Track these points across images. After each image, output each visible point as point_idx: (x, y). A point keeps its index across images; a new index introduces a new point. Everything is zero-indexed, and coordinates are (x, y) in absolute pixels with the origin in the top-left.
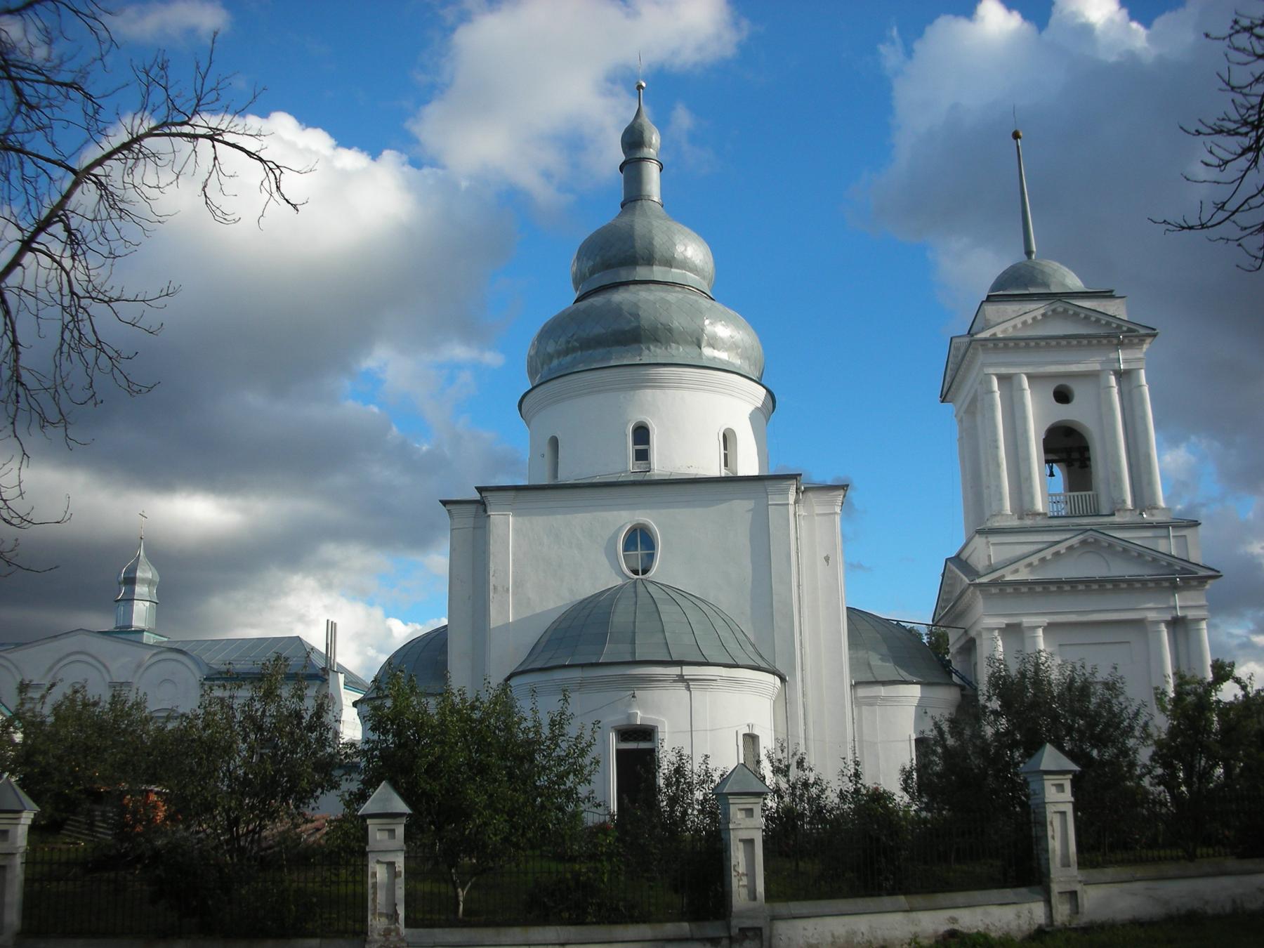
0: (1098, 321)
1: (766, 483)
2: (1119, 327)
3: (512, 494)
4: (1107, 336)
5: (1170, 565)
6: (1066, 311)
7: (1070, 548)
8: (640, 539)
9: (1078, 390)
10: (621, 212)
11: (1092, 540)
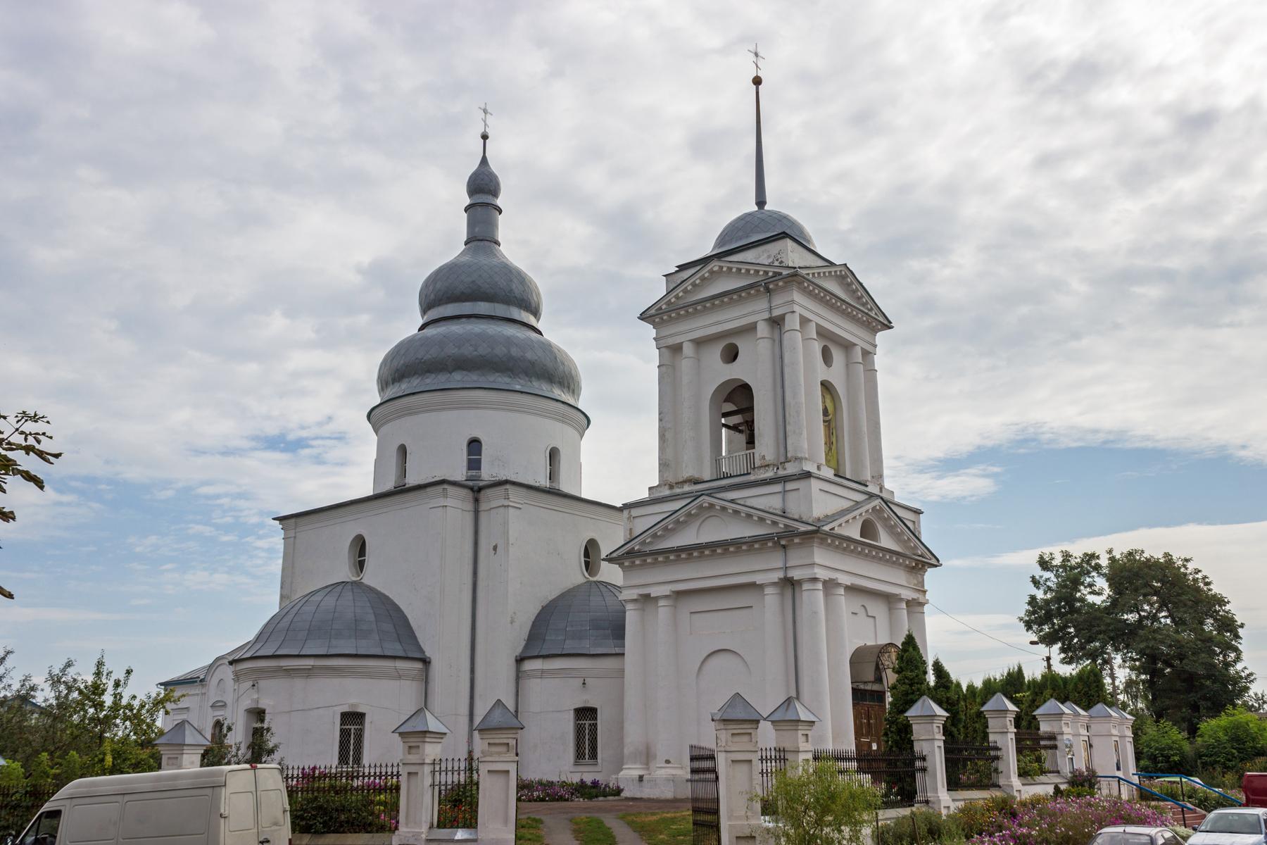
0: (748, 271)
1: (428, 489)
2: (766, 273)
3: (293, 520)
4: (751, 286)
5: (775, 523)
6: (721, 267)
7: (689, 515)
8: (360, 546)
10: (465, 249)
11: (707, 505)
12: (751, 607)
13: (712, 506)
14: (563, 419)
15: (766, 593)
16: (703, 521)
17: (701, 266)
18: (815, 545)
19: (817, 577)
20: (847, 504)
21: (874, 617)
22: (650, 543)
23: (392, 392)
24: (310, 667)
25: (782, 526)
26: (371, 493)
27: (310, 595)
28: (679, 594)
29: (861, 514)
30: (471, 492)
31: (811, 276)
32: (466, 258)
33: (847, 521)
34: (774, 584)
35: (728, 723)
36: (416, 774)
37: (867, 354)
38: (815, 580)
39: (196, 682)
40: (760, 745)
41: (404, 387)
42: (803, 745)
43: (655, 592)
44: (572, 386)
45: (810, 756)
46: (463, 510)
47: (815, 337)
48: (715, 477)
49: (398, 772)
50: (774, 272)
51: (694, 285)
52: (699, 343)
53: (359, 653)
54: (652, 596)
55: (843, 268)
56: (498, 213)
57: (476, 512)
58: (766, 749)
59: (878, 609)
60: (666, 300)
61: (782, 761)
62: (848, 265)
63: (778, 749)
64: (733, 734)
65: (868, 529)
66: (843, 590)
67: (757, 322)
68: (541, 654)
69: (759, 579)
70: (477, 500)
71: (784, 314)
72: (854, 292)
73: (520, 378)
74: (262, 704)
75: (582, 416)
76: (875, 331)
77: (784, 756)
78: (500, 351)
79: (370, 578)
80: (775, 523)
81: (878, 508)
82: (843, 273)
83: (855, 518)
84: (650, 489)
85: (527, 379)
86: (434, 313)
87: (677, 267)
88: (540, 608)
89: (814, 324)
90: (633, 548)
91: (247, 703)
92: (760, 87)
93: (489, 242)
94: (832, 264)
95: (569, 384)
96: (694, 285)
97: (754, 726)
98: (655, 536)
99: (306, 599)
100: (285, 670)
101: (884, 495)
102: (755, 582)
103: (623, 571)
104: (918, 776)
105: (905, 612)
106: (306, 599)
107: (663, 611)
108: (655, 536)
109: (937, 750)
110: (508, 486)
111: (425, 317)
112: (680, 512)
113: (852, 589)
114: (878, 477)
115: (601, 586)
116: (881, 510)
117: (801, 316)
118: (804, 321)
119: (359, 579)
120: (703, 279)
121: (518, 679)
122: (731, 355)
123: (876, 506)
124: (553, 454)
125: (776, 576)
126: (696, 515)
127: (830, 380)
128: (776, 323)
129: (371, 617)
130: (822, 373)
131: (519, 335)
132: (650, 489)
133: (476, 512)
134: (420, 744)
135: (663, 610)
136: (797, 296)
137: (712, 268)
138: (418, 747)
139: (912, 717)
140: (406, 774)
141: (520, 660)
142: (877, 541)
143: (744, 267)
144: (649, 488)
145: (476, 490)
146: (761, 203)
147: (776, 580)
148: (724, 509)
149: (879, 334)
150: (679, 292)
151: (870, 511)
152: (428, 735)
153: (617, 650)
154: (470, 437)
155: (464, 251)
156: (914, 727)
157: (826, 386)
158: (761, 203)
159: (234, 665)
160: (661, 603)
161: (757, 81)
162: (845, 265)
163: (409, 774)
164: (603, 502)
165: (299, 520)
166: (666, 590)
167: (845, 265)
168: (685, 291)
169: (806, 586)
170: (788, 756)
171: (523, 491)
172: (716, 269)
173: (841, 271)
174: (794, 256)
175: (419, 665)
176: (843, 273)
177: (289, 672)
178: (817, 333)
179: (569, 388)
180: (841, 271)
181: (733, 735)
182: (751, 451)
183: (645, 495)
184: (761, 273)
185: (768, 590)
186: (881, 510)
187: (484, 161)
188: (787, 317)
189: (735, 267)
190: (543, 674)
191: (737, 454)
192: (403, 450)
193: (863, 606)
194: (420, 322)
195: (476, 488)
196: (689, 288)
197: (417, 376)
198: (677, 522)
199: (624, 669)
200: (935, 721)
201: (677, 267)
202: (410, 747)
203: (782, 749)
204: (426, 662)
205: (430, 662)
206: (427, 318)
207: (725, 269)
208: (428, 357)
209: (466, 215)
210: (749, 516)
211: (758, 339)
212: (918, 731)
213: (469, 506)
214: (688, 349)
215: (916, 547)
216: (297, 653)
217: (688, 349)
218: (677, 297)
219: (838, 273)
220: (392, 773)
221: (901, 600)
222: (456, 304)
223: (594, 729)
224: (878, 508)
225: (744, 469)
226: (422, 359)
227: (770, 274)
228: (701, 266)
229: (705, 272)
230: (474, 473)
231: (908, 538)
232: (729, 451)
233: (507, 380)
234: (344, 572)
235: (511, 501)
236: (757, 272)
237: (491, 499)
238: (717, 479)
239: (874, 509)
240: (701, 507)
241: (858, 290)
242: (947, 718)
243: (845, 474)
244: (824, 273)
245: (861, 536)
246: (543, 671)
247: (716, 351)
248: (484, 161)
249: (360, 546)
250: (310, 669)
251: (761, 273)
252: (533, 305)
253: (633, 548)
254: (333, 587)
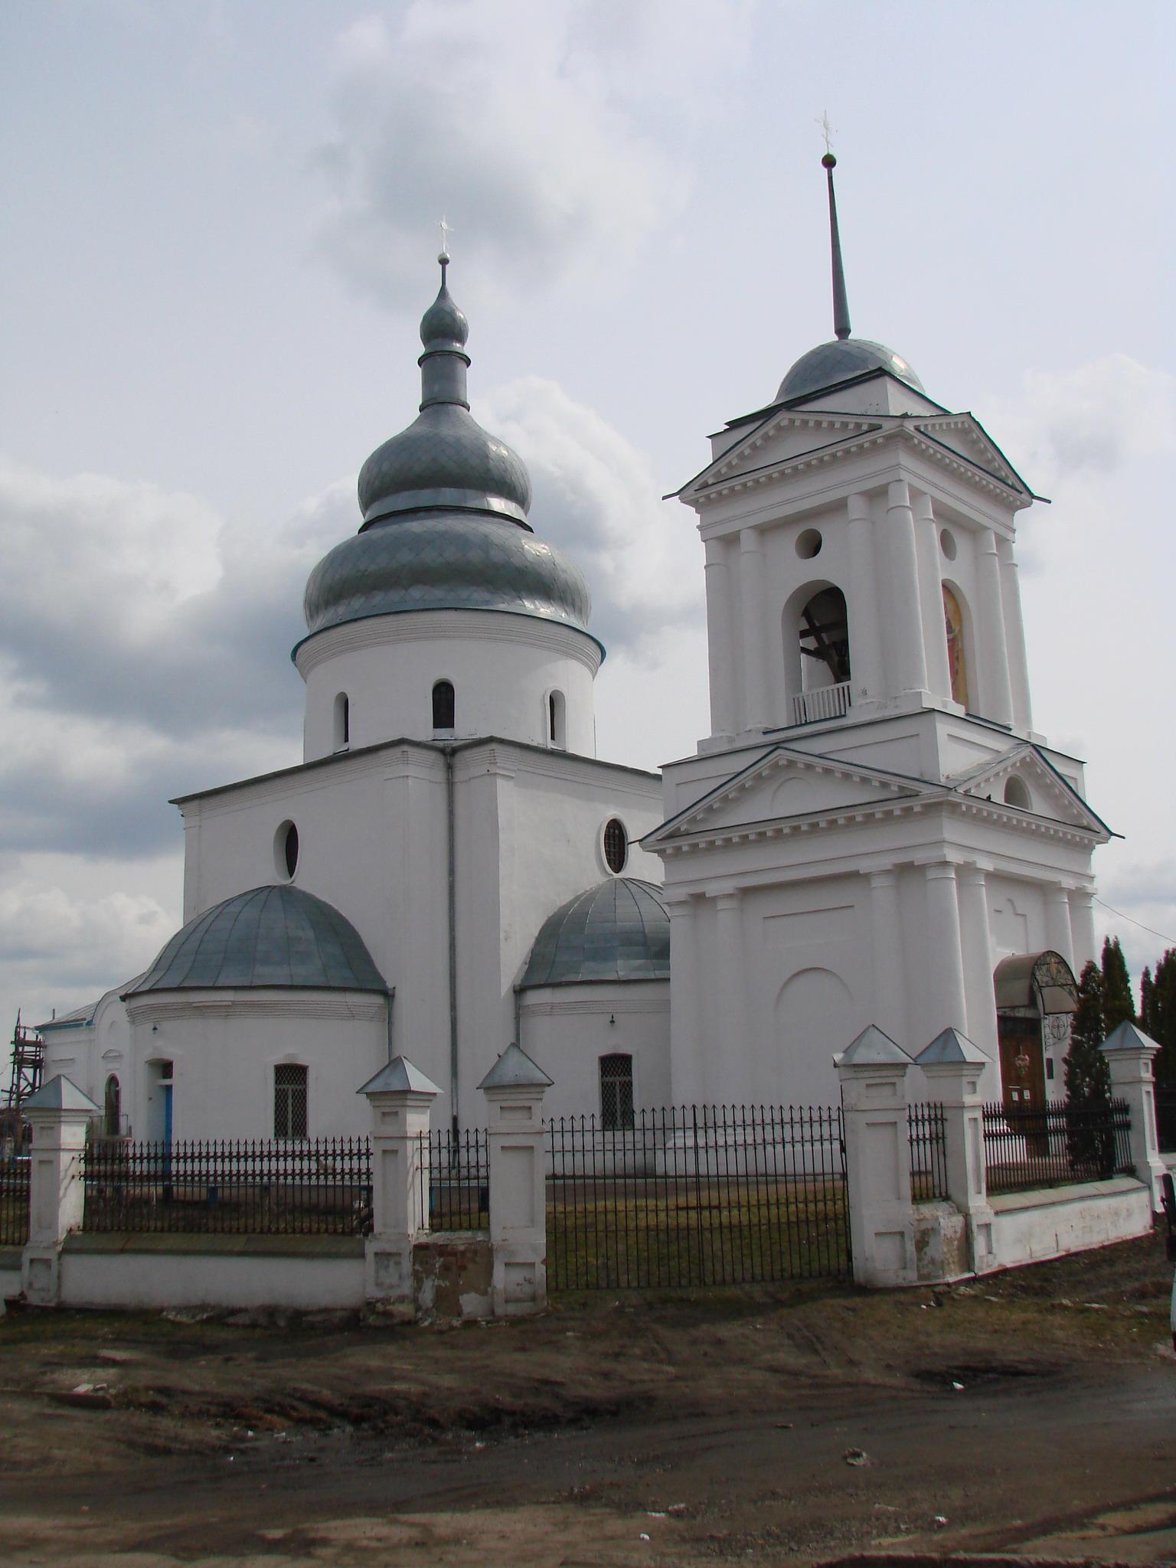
0: (832, 424)
1: (383, 753)
2: (858, 426)
3: (196, 803)
5: (884, 785)
6: (792, 421)
7: (759, 777)
8: (290, 840)
9: (828, 531)
11: (785, 762)
12: (853, 906)
13: (791, 764)
14: (570, 653)
15: (873, 886)
16: (781, 784)
17: (760, 422)
18: (943, 814)
19: (948, 860)
20: (986, 757)
21: (1023, 915)
22: (702, 821)
23: (320, 622)
24: (230, 1003)
25: (896, 789)
26: (299, 761)
27: (225, 904)
28: (746, 892)
29: (1005, 769)
30: (442, 756)
32: (424, 429)
33: (987, 780)
34: (887, 872)
35: (860, 1069)
36: (395, 1152)
37: (1003, 542)
38: (945, 864)
39: (81, 1025)
40: (909, 1100)
41: (341, 611)
42: (968, 1099)
43: (711, 889)
44: (578, 603)
45: (979, 1114)
46: (430, 782)
47: (932, 517)
48: (794, 724)
49: (368, 1150)
51: (754, 447)
52: (764, 530)
53: (295, 984)
54: (707, 896)
55: (966, 418)
56: (465, 365)
57: (450, 785)
58: (916, 1106)
59: (1028, 904)
60: (713, 472)
61: (940, 1122)
62: (973, 415)
63: (932, 1105)
64: (868, 1086)
65: (1014, 793)
66: (983, 878)
67: (847, 497)
68: (550, 981)
69: (864, 866)
70: (450, 768)
71: (890, 483)
72: (982, 452)
73: (505, 594)
74: (169, 1052)
75: (593, 646)
76: (1012, 508)
77: (942, 1115)
78: (475, 556)
79: (305, 879)
80: (884, 785)
81: (1028, 759)
82: (967, 426)
83: (997, 774)
84: (700, 743)
85: (514, 593)
86: (379, 508)
87: (726, 424)
88: (546, 919)
89: (930, 499)
91: (148, 1054)
92: (833, 170)
93: (454, 406)
94: (946, 413)
95: (573, 600)
96: (754, 447)
97: (900, 1073)
98: (710, 809)
99: (220, 909)
100: (195, 1007)
101: (1034, 741)
103: (664, 862)
104: (1118, 1135)
105: (1067, 906)
106: (220, 909)
107: (726, 917)
108: (710, 809)
109: (1144, 1096)
110: (494, 746)
111: (368, 514)
112: (744, 775)
113: (994, 877)
114: (1025, 717)
115: (630, 886)
116: (1033, 763)
117: (911, 488)
118: (916, 494)
119: (290, 881)
120: (766, 438)
121: (517, 1018)
122: (812, 545)
123: (1025, 757)
124: (555, 702)
125: (887, 862)
126: (770, 777)
127: (954, 580)
128: (877, 495)
129: (310, 934)
130: (943, 570)
131: (501, 532)
132: (700, 743)
133: (450, 785)
134: (398, 1109)
135: (726, 917)
136: (905, 459)
137: (778, 424)
138: (396, 1113)
139: (1108, 1050)
140: (381, 1152)
141: (519, 991)
142: (1027, 809)
143: (825, 420)
144: (698, 742)
145: (449, 754)
146: (842, 330)
147: (889, 867)
148: (809, 767)
149: (1018, 513)
150: (732, 457)
151: (1018, 764)
152: (409, 1097)
153: (658, 974)
154: (439, 678)
155: (419, 418)
156: (1112, 1066)
157: (949, 589)
158: (842, 330)
159: (127, 1001)
160: (721, 905)
161: (829, 162)
162: (970, 413)
163: (385, 1152)
164: (630, 766)
165: (205, 802)
166: (728, 886)
167: (970, 413)
168: (742, 457)
169: (932, 874)
170: (947, 1114)
171: (516, 753)
172: (785, 423)
173: (963, 423)
174: (897, 403)
175: (378, 1000)
176: (967, 426)
177: (201, 1010)
178: (935, 513)
179: (573, 605)
180: (963, 423)
181: (868, 1086)
182: (844, 684)
183: (692, 752)
184: (851, 426)
185: (877, 882)
186: (1033, 763)
187: (443, 293)
188: (892, 488)
189: (812, 420)
190: (552, 1009)
191: (821, 689)
192: (344, 703)
193: (1009, 900)
194: (360, 520)
195: (448, 750)
196: (747, 452)
197: (359, 595)
198: (742, 788)
199: (669, 1000)
200: (1142, 1056)
201: (726, 424)
202: (384, 1114)
203: (938, 1105)
204: (388, 995)
205: (393, 996)
206: (370, 515)
207: (797, 423)
208: (372, 568)
209: (420, 369)
210: (847, 776)
211: (850, 522)
212: (1118, 1070)
213: (440, 775)
214: (748, 541)
215: (1080, 816)
216: (211, 985)
217: (748, 541)
218: (729, 465)
219: (960, 426)
220: (359, 1150)
221: (1062, 889)
222: (411, 493)
223: (628, 1087)
224: (1028, 759)
225: (835, 710)
226: (366, 570)
227: (865, 428)
228: (760, 422)
229: (769, 427)
230: (443, 733)
231: (1069, 802)
232: (810, 688)
233: (486, 596)
234: (267, 872)
235: (498, 767)
236: (845, 425)
237: (470, 765)
238: (797, 726)
240: (775, 766)
242: (1158, 1050)
244: (941, 425)
245: (1006, 801)
246: (553, 1006)
247: (787, 543)
248: (443, 293)
249: (290, 840)
250: (229, 1006)
251: (851, 426)
252: (519, 491)
254: (256, 893)
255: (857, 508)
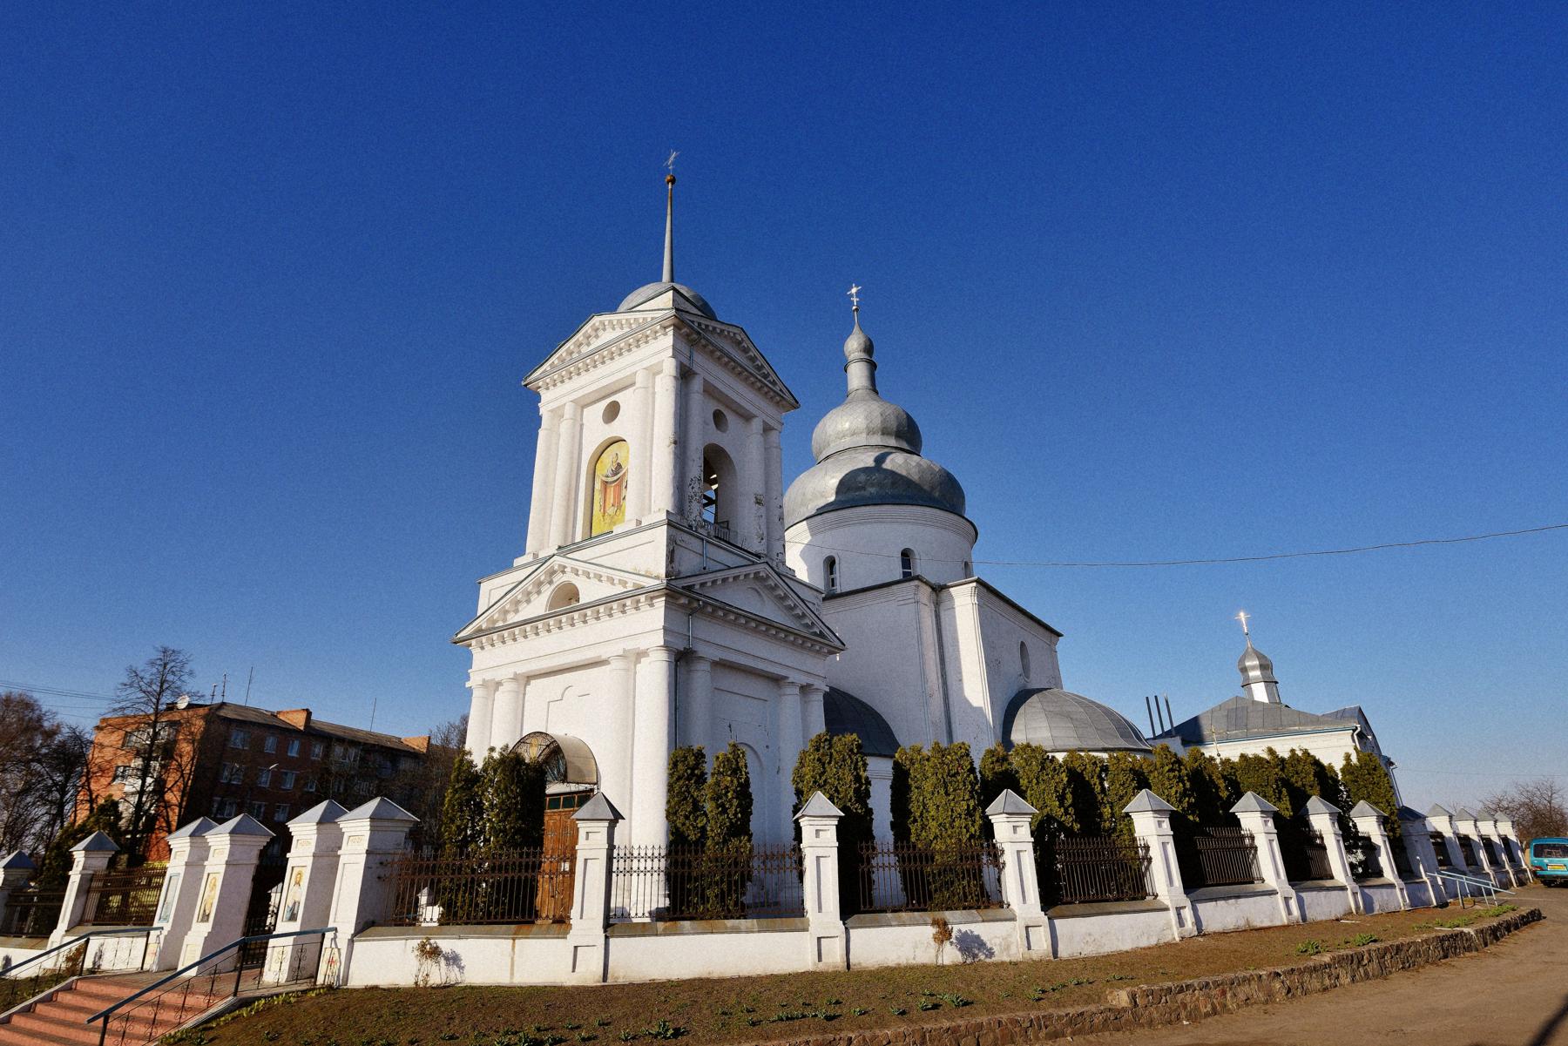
31: (696, 324)
50: (652, 319)
52: (583, 404)
90: (481, 626)
102: (600, 656)
122: (612, 412)
125: (617, 649)
151: (752, 576)
227: (649, 320)
239: (757, 574)
241: (750, 349)
243: (737, 542)
253: (481, 626)
255: (639, 380)
